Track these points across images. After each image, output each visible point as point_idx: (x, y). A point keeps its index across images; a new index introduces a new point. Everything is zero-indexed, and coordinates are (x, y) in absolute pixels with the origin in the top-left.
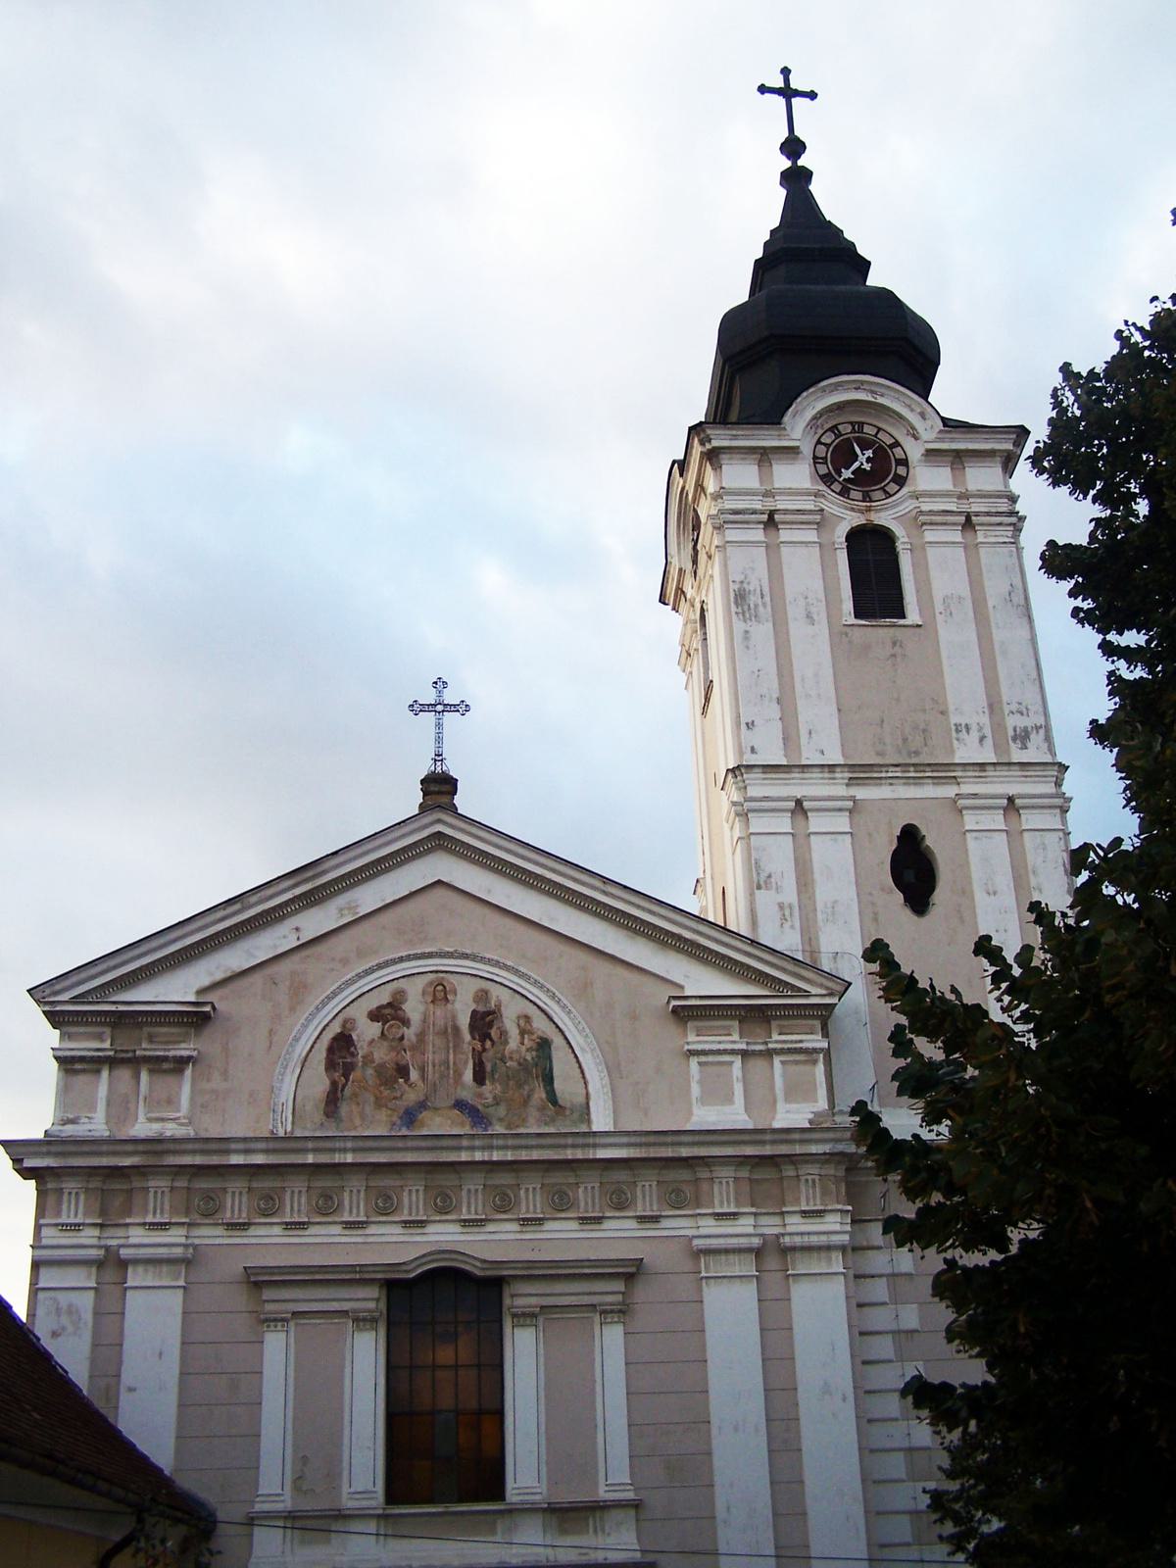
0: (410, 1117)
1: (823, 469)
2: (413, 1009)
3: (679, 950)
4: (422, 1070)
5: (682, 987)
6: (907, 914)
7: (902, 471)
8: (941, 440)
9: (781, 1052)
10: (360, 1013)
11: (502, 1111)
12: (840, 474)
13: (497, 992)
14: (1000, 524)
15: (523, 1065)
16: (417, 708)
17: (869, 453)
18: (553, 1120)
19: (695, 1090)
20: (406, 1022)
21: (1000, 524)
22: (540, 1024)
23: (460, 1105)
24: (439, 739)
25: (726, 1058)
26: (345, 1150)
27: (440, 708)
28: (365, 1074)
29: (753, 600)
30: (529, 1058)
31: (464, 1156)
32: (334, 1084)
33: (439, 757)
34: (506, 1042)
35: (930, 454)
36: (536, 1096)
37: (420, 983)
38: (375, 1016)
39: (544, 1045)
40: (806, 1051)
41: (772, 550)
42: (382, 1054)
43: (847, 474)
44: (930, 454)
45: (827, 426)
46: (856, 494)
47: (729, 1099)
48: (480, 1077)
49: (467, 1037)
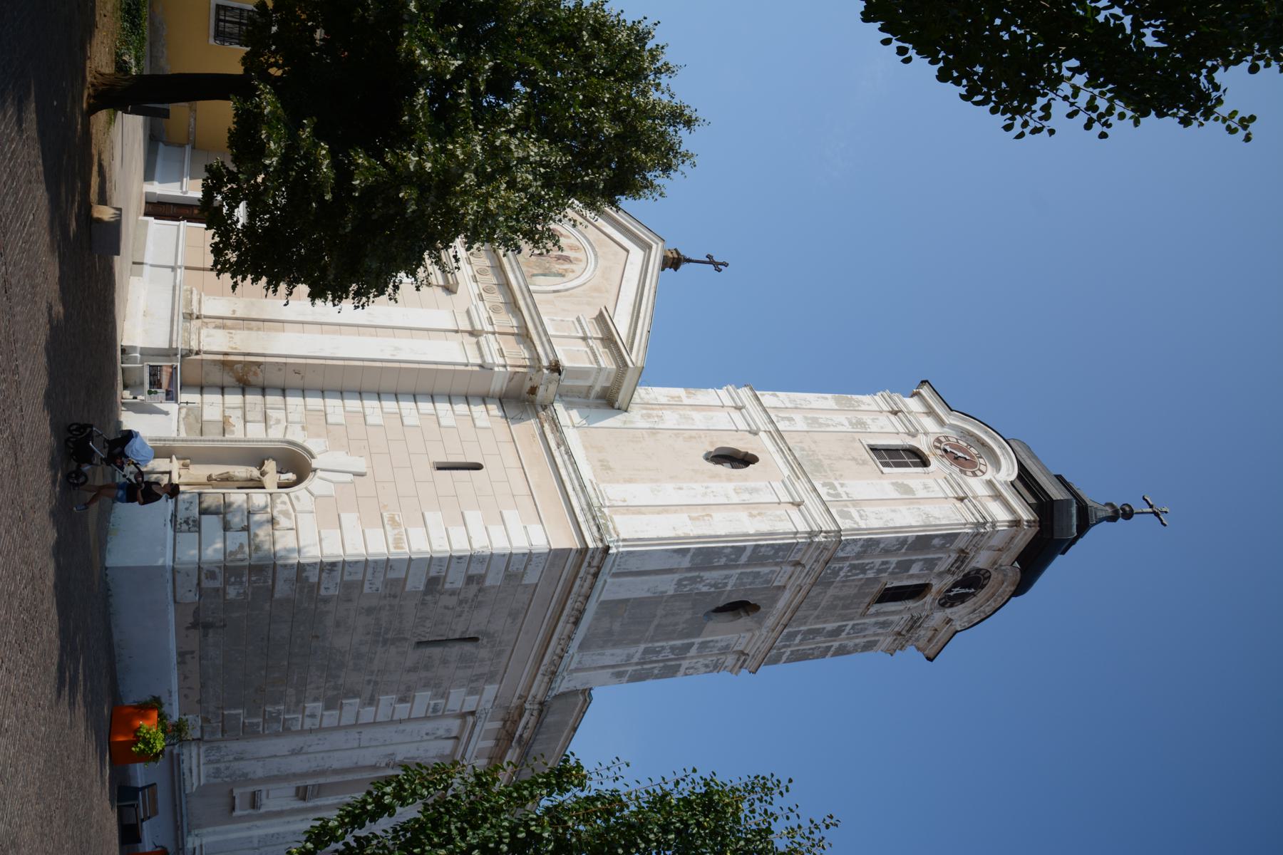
8: (1001, 484)
14: (973, 514)
21: (973, 514)
22: (571, 275)
35: (990, 484)
37: (578, 243)
44: (990, 484)
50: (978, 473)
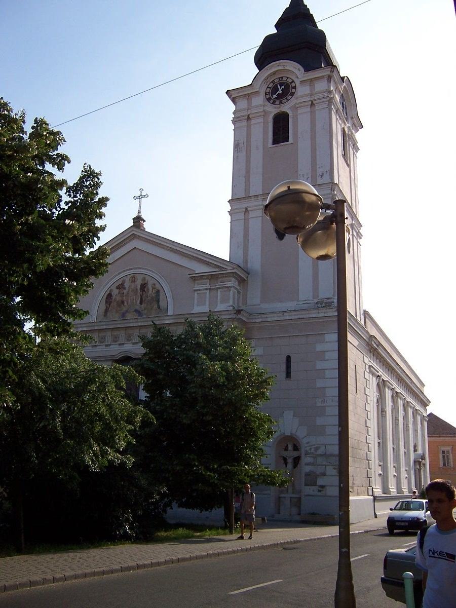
0: (123, 315)
1: (268, 96)
2: (127, 285)
3: (195, 260)
4: (128, 302)
5: (195, 271)
6: (277, 240)
7: (293, 91)
8: (303, 77)
9: (219, 288)
10: (114, 287)
11: (146, 311)
12: (272, 96)
13: (147, 278)
15: (152, 298)
16: (135, 198)
17: (283, 87)
18: (158, 313)
19: (196, 302)
20: (125, 289)
22: (158, 286)
23: (136, 311)
24: (140, 206)
25: (205, 291)
26: (104, 325)
27: (141, 197)
28: (114, 304)
29: (241, 145)
30: (154, 295)
31: (132, 325)
32: (107, 307)
33: (139, 211)
34: (148, 292)
36: (155, 306)
37: (129, 277)
38: (118, 288)
39: (158, 291)
40: (226, 287)
41: (249, 128)
42: (118, 298)
43: (275, 96)
45: (270, 81)
46: (277, 103)
47: (204, 304)
48: (141, 303)
49: (139, 291)
50: (293, 85)
